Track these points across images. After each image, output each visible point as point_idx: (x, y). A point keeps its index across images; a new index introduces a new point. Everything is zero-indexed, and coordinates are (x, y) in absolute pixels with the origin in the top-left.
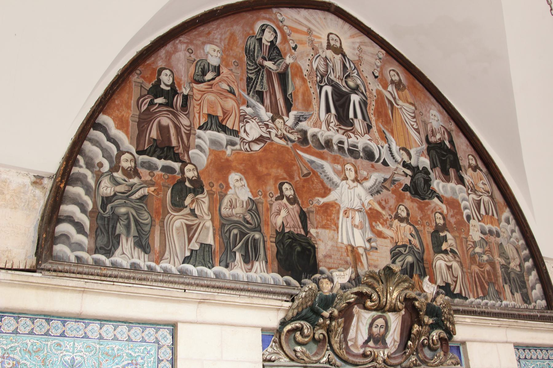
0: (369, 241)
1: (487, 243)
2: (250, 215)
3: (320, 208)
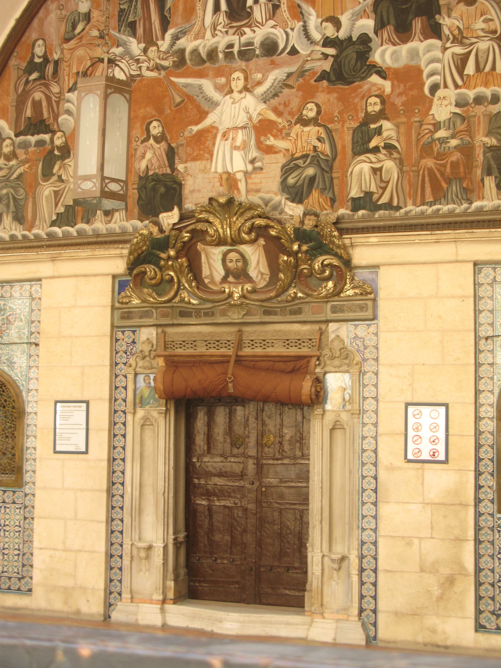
0: (252, 161)
1: (463, 119)
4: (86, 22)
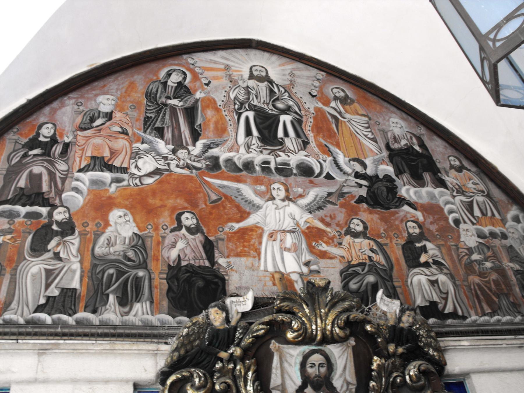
0: (307, 264)
1: (488, 248)
2: (133, 251)
3: (233, 235)
4: (106, 119)
